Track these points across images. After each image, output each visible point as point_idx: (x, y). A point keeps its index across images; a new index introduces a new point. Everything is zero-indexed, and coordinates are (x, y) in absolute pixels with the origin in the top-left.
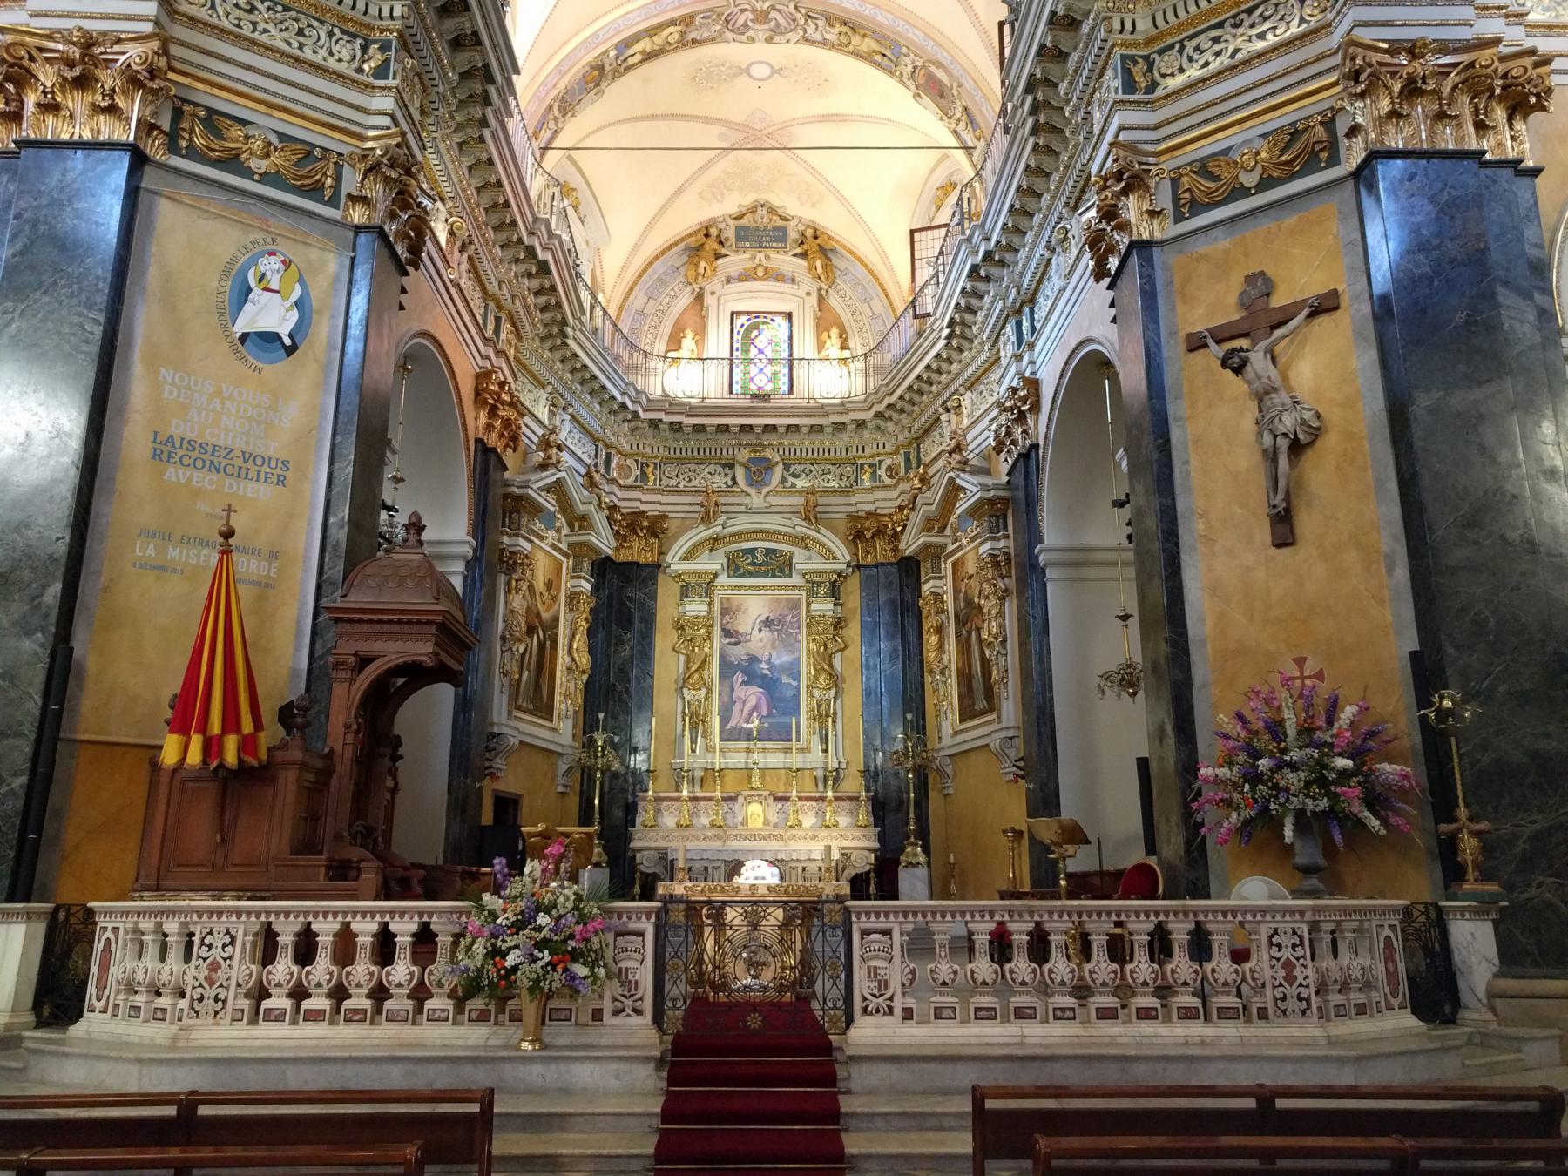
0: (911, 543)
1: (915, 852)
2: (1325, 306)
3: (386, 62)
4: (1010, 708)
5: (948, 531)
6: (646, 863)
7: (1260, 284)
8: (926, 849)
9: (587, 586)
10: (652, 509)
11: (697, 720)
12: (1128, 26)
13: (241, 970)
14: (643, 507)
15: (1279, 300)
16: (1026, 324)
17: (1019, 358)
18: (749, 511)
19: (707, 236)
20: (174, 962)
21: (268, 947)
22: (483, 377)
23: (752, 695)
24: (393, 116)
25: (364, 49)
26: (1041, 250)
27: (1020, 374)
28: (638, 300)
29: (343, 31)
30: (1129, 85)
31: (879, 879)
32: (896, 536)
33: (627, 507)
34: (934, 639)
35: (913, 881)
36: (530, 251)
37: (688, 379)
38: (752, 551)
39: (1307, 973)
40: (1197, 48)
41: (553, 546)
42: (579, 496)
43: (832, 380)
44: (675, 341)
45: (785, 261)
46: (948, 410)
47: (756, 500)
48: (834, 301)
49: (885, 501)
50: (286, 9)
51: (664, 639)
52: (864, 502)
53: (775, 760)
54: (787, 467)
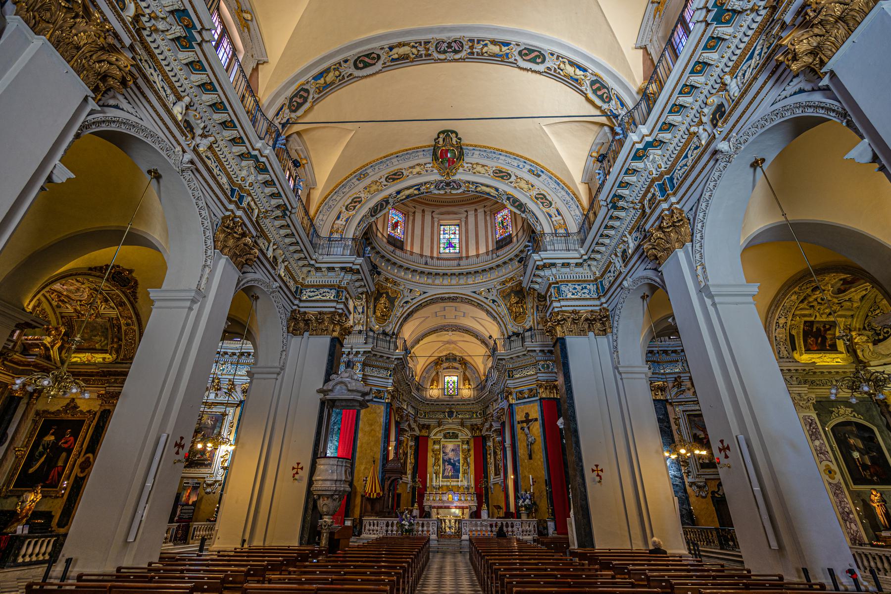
0: (484, 433)
1: (485, 506)
2: (536, 420)
4: (502, 474)
6: (426, 509)
8: (488, 506)
10: (427, 423)
11: (437, 474)
13: (385, 528)
20: (376, 527)
21: (387, 525)
23: (449, 467)
28: (424, 374)
31: (476, 515)
32: (481, 431)
33: (422, 423)
35: (484, 514)
37: (434, 392)
39: (520, 529)
42: (412, 422)
43: (467, 392)
44: (432, 384)
45: (456, 365)
47: (450, 421)
48: (467, 373)
49: (479, 421)
51: (430, 454)
52: (474, 421)
53: (455, 484)
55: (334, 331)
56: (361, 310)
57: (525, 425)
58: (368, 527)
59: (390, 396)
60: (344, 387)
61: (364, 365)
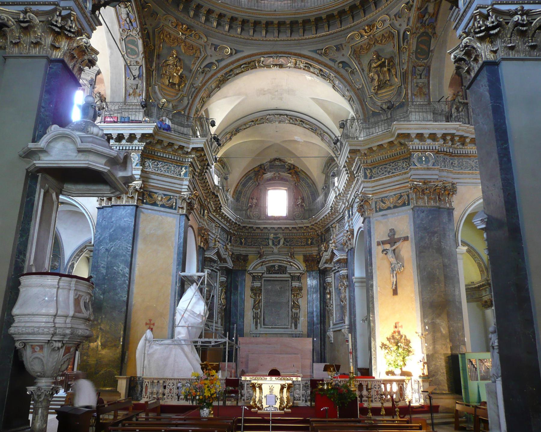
0: (321, 266)
2: (406, 239)
3: (186, 172)
5: (333, 263)
7: (393, 232)
9: (225, 279)
10: (244, 253)
12: (365, 162)
14: (241, 252)
15: (396, 237)
16: (351, 212)
17: (349, 222)
18: (273, 253)
19: (261, 167)
22: (200, 229)
24: (188, 186)
25: (181, 169)
26: (352, 197)
27: (349, 226)
29: (177, 165)
30: (365, 176)
32: (318, 262)
34: (328, 296)
36: (214, 193)
38: (274, 266)
40: (381, 169)
41: (216, 269)
45: (285, 175)
46: (332, 227)
47: (276, 250)
50: (165, 163)
54: (285, 239)
55: (54, 47)
56: (136, 73)
57: (387, 246)
58: (149, 390)
59: (185, 205)
60: (71, 146)
61: (145, 156)
